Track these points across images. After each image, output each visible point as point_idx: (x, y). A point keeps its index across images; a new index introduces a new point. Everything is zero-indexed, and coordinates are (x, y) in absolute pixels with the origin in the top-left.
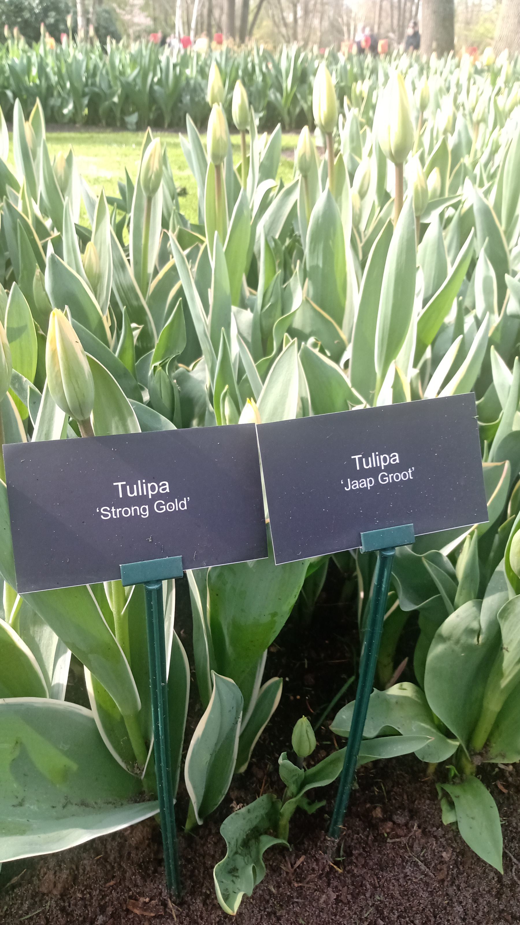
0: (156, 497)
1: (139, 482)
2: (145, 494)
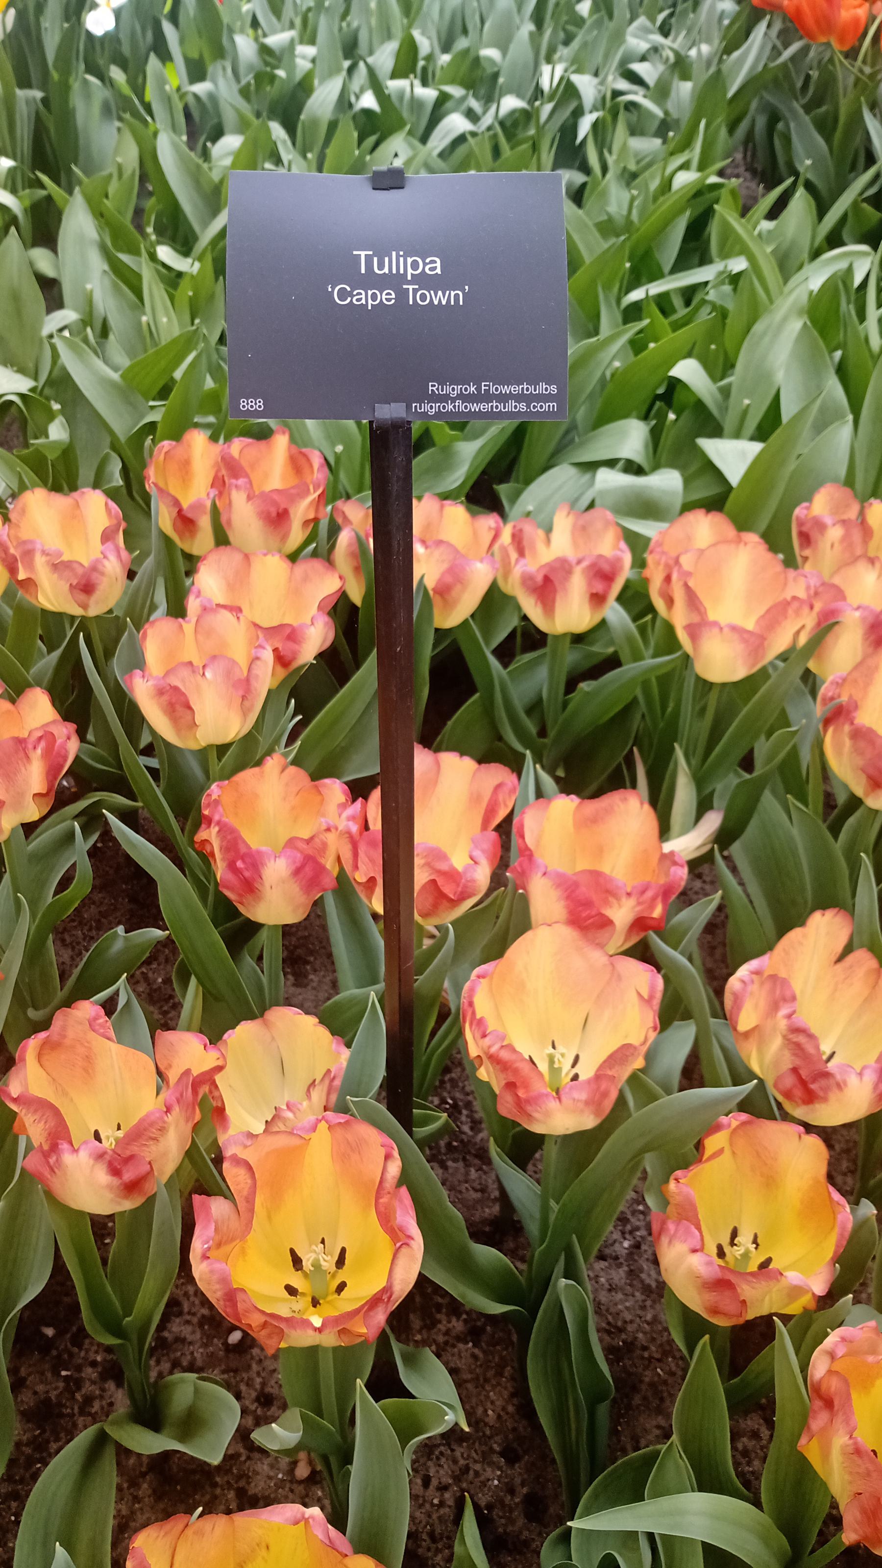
1: (394, 253)
2: (402, 272)
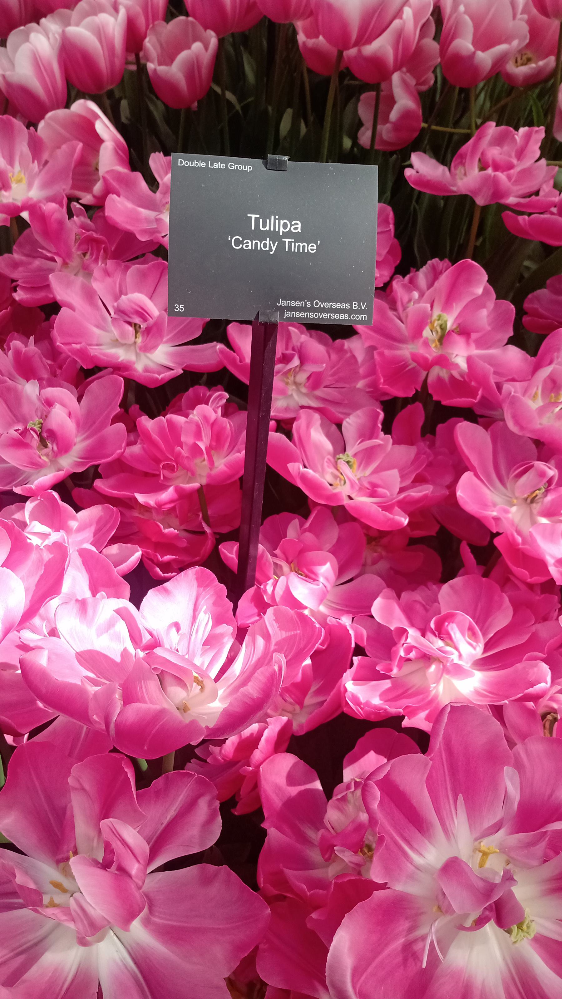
0: (286, 235)
1: (273, 217)
2: (277, 230)
